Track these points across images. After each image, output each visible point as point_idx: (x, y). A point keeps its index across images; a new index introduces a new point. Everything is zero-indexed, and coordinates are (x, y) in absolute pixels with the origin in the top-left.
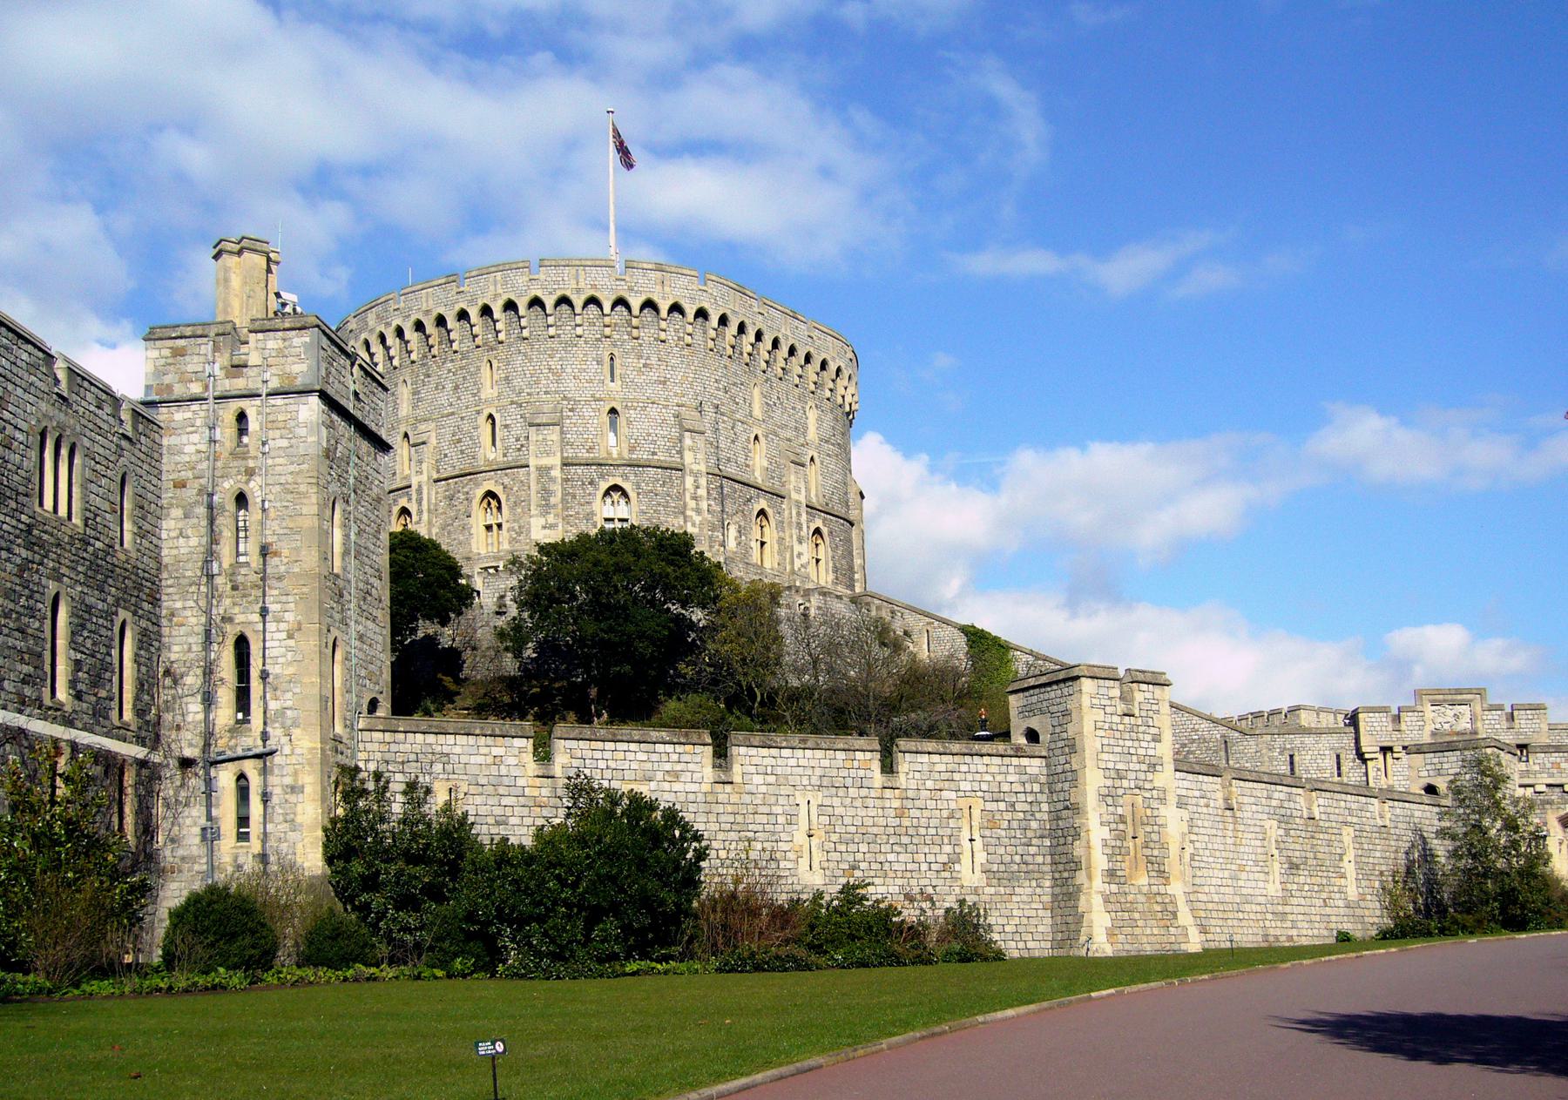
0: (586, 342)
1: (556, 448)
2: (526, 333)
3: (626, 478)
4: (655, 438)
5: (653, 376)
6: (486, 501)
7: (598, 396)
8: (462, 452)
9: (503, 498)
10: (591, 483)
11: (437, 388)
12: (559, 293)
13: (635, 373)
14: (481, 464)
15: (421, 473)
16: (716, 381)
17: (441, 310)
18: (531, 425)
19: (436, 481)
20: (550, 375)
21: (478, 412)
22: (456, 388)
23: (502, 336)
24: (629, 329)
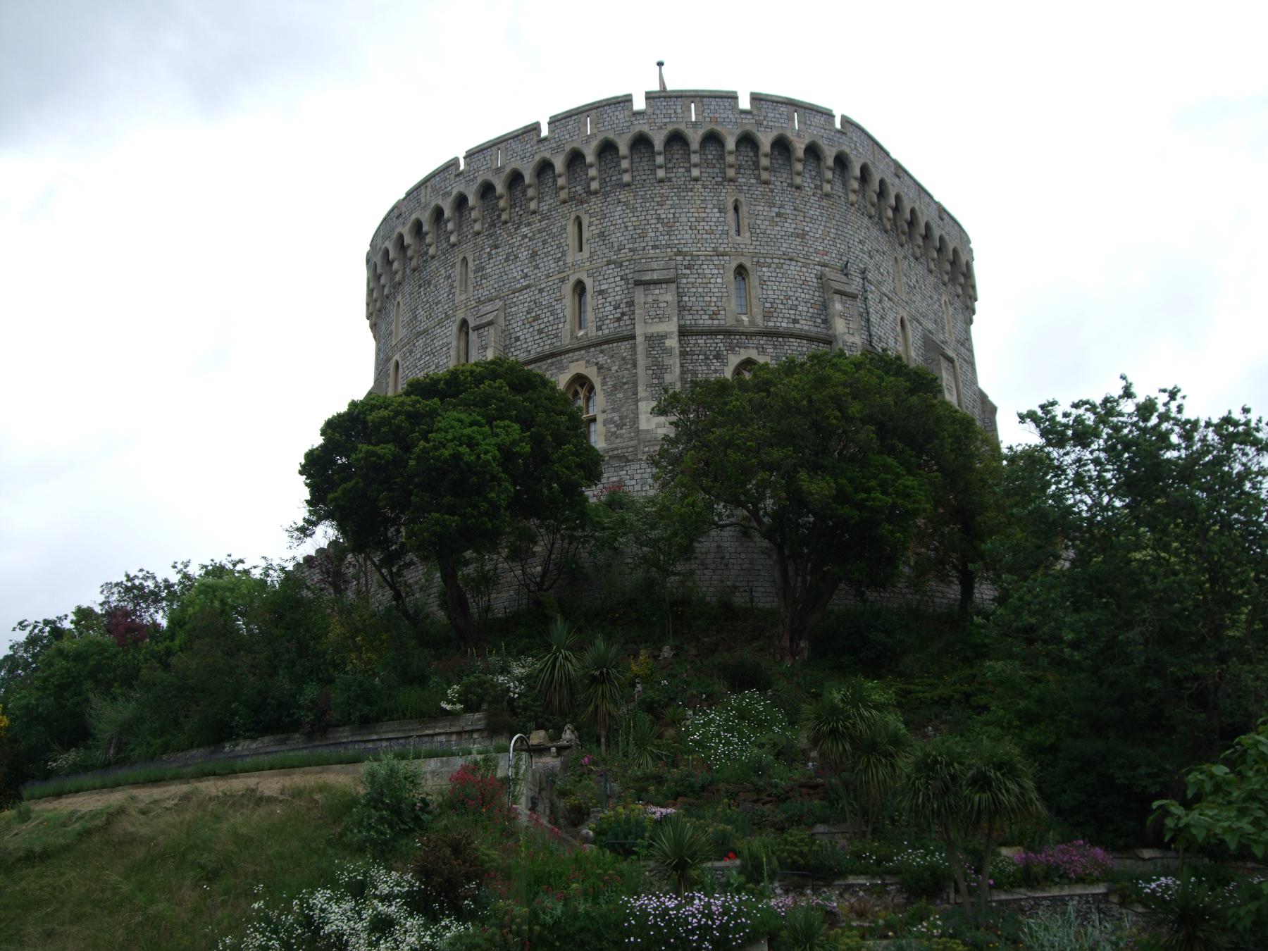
0: (704, 187)
2: (627, 178)
4: (795, 303)
5: (789, 226)
7: (721, 249)
8: (540, 332)
9: (597, 381)
10: (718, 357)
11: (507, 260)
12: (670, 128)
13: (767, 223)
14: (566, 341)
16: (860, 242)
17: (516, 164)
18: (638, 283)
20: (659, 225)
21: (563, 280)
22: (534, 255)
23: (595, 185)
24: (756, 172)
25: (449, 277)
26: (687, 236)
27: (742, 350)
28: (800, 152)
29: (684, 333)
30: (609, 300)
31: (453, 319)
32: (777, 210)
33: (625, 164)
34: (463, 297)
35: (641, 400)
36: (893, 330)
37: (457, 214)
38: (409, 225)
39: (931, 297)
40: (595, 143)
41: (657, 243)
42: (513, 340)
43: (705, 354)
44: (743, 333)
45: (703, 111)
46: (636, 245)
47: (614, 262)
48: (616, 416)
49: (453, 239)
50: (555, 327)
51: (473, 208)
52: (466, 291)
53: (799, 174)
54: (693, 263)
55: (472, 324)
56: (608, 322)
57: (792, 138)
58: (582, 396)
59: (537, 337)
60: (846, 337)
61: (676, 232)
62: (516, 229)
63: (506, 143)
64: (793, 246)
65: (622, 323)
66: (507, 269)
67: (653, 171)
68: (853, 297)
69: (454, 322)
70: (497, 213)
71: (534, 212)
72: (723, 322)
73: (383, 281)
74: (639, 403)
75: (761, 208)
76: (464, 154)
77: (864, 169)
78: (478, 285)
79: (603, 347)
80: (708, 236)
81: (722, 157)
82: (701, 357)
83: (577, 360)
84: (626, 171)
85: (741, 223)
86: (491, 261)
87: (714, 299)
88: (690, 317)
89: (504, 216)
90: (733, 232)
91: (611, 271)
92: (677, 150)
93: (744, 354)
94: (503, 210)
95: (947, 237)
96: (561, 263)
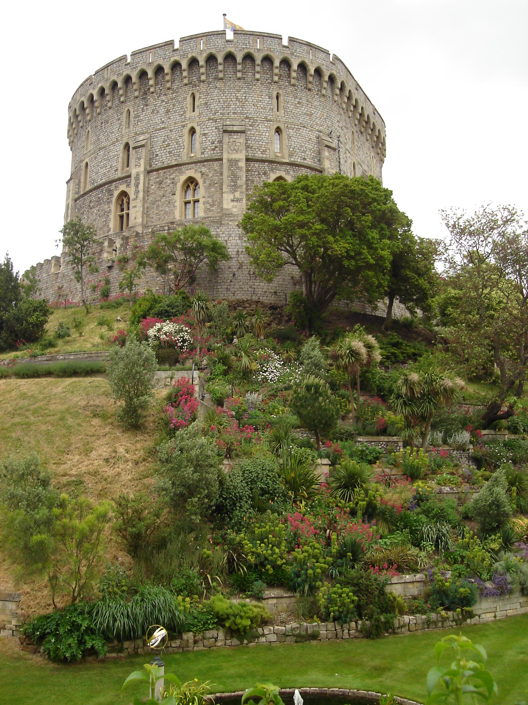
1: (243, 147)
2: (221, 75)
3: (288, 173)
4: (305, 149)
5: (304, 110)
6: (186, 185)
7: (269, 118)
8: (170, 152)
9: (200, 181)
10: (265, 174)
11: (152, 112)
12: (246, 51)
13: (293, 106)
14: (185, 159)
15: (139, 166)
16: (338, 121)
17: (161, 62)
18: (225, 131)
19: (152, 171)
20: (237, 102)
21: (183, 126)
22: (168, 111)
24: (289, 79)
25: (119, 119)
26: (251, 109)
27: (277, 171)
28: (312, 71)
29: (248, 160)
30: (208, 139)
31: (121, 142)
32: (298, 100)
33: (220, 68)
34: (127, 130)
35: (225, 192)
36: (350, 168)
37: (125, 86)
38: (97, 89)
39: (367, 153)
40: (205, 55)
41: (236, 111)
42: (154, 156)
43: (258, 172)
44: (278, 163)
45: (264, 44)
46: (225, 111)
47: (212, 119)
48: (210, 200)
49: (122, 99)
50: (178, 151)
51: (134, 84)
52: (129, 127)
53: (310, 83)
54: (254, 123)
55: (132, 145)
56: (206, 150)
57: (308, 63)
58: (192, 188)
59: (168, 155)
60: (329, 170)
61: (246, 107)
62: (158, 97)
63: (154, 50)
64: (305, 120)
65: (215, 152)
66: (152, 117)
67: (236, 72)
68: (334, 149)
69: (121, 143)
70: (148, 87)
71: (169, 89)
72: (268, 156)
73: (79, 118)
74: (224, 195)
75: (290, 99)
76: (131, 54)
77: (342, 84)
78: (135, 125)
79: (205, 163)
80: (262, 110)
81: (271, 69)
82: (256, 173)
83: (190, 169)
84: (221, 71)
85: (279, 105)
86: (144, 113)
87: (264, 144)
88: (251, 152)
89: (152, 90)
90: (275, 109)
91: (210, 123)
92: (248, 62)
93: (278, 174)
94: (152, 86)
95: (376, 123)
96: (183, 117)
